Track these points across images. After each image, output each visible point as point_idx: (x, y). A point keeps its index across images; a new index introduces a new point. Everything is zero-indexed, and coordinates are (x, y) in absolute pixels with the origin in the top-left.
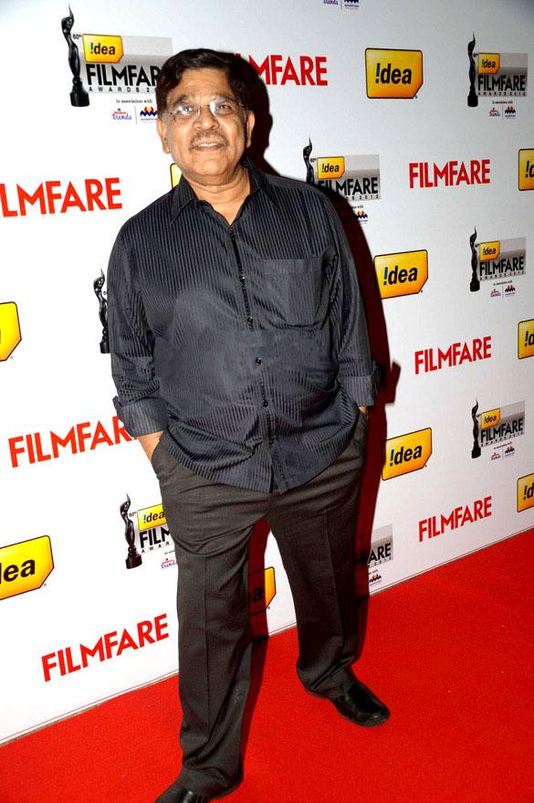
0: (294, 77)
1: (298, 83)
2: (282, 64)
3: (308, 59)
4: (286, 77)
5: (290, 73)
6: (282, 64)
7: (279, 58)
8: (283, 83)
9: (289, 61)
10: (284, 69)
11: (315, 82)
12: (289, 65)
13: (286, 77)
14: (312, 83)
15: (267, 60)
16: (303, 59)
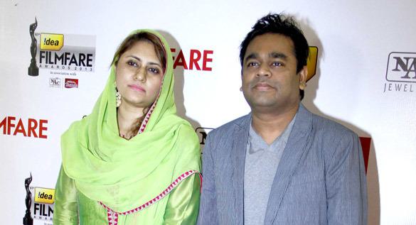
0: (23, 131)
1: (25, 135)
2: (15, 122)
3: (35, 121)
4: (17, 131)
5: (20, 128)
6: (15, 122)
7: (14, 119)
8: (15, 134)
9: (20, 121)
10: (16, 126)
11: (38, 135)
12: (20, 123)
13: (17, 131)
14: (35, 136)
15: (5, 119)
16: (30, 120)
